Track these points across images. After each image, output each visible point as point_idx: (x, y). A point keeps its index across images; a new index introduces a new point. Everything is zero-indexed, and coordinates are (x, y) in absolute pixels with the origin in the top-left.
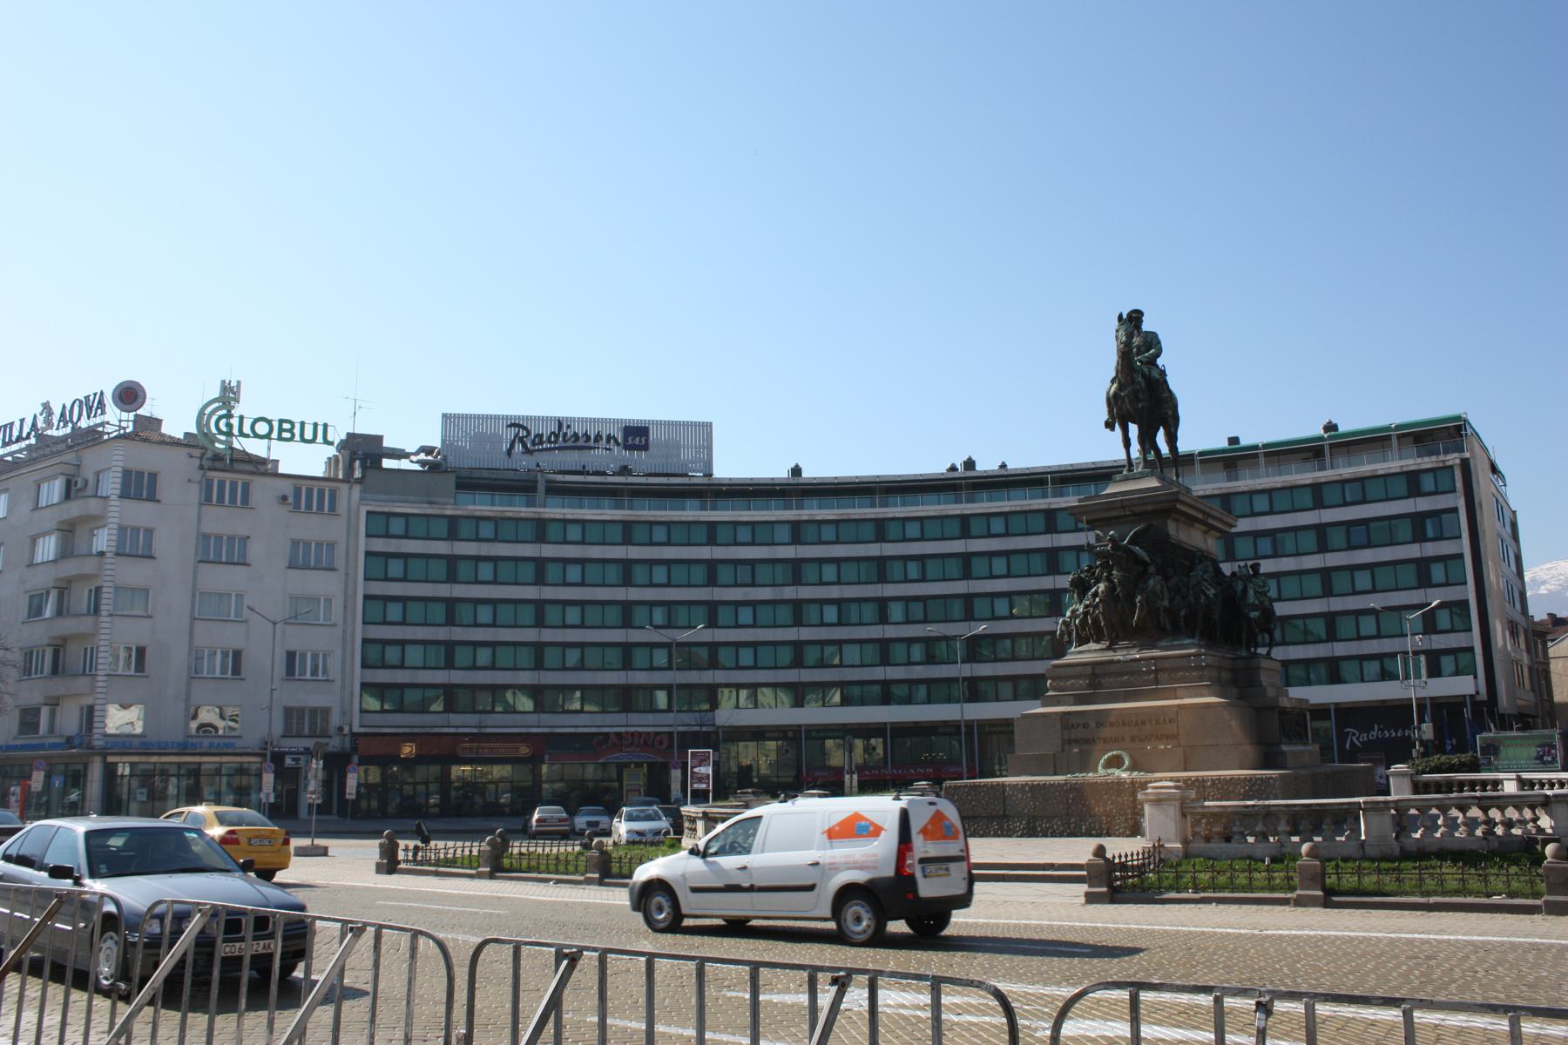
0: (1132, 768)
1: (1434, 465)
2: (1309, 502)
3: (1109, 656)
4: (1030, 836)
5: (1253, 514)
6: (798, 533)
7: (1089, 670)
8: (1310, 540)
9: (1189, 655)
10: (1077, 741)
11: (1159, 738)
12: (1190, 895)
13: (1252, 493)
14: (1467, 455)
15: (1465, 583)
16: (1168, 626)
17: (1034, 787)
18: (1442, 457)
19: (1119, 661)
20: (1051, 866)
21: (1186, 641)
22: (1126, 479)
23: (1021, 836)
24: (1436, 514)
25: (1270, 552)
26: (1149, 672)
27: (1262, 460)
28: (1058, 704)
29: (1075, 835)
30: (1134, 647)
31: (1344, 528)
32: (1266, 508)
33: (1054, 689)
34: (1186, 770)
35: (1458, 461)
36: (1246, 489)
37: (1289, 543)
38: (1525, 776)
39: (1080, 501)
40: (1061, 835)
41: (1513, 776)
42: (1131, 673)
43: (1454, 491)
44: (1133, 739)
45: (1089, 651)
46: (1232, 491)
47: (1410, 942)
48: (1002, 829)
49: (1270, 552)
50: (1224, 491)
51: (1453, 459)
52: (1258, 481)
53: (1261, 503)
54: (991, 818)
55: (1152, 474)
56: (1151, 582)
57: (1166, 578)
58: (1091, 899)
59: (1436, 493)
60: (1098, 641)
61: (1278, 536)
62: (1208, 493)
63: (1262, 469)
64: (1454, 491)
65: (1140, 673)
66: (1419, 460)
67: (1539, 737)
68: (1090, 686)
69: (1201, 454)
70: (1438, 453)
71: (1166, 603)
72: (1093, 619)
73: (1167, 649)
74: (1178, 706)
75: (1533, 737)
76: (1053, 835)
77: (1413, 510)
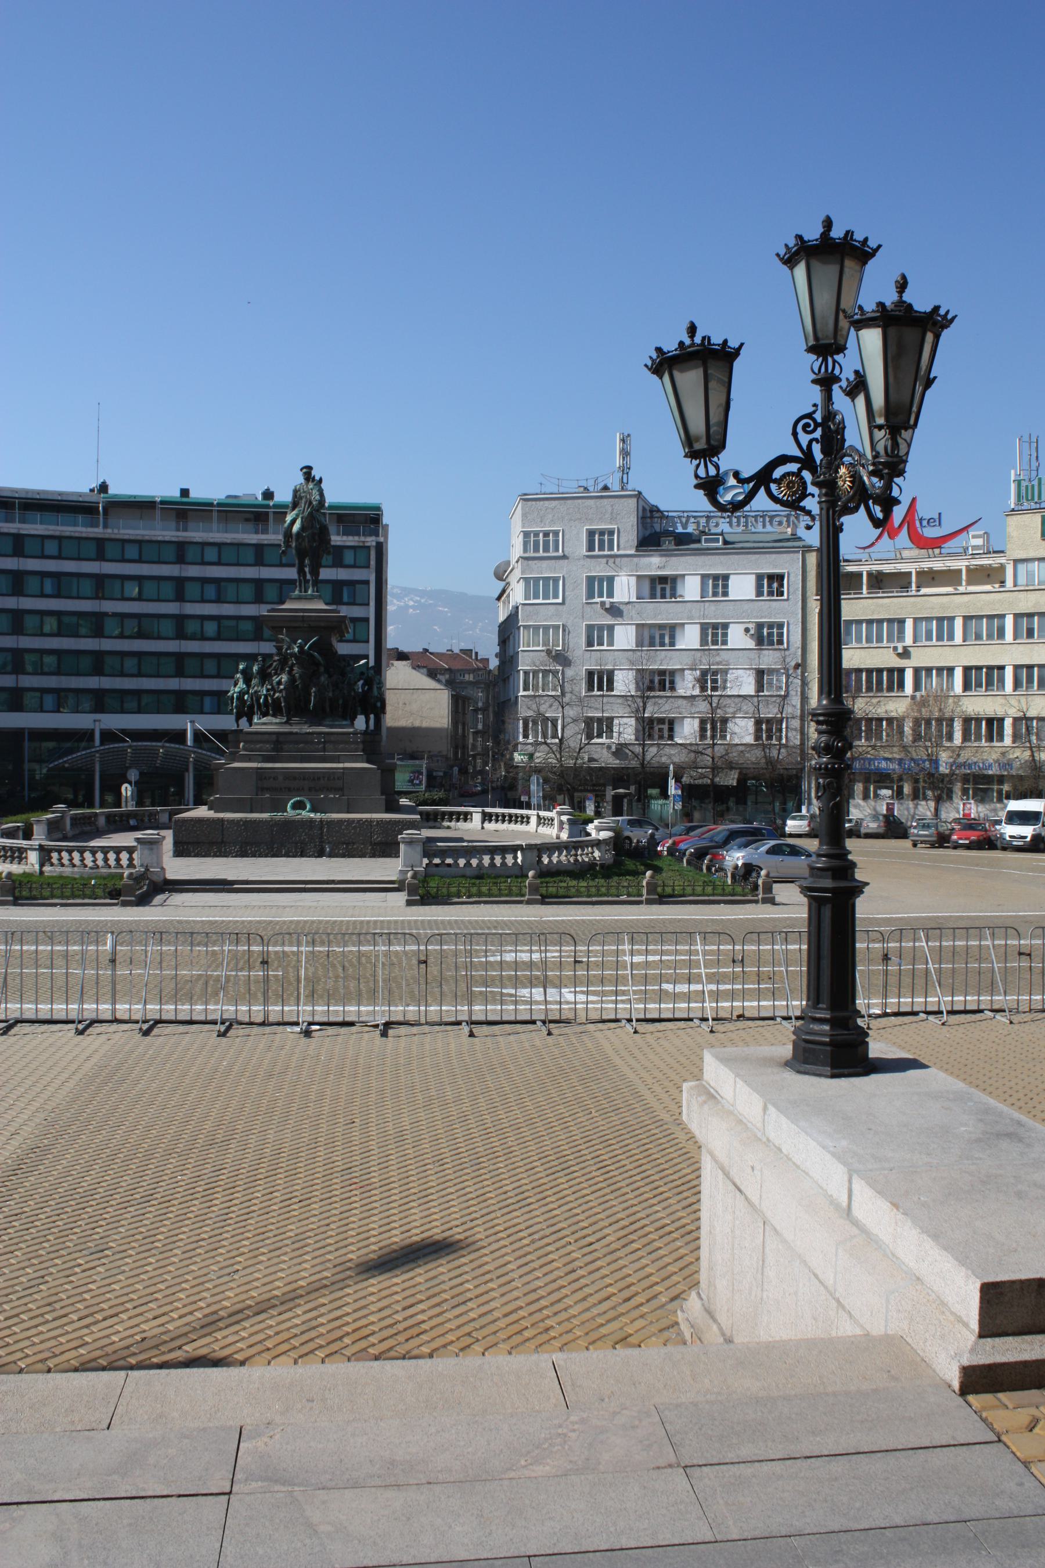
0: (313, 810)
1: (356, 544)
2: (251, 559)
3: (286, 729)
4: (243, 856)
5: (203, 563)
7: (274, 737)
8: (248, 591)
9: (349, 733)
10: (268, 789)
11: (330, 790)
12: (464, 899)
13: (204, 544)
14: (381, 539)
15: (367, 641)
16: (328, 710)
17: (247, 823)
18: (362, 539)
19: (296, 733)
20: (333, 882)
21: (344, 723)
22: (299, 598)
23: (236, 856)
24: (352, 583)
25: (213, 598)
26: (319, 742)
27: (215, 515)
28: (250, 760)
29: (277, 856)
30: (306, 723)
31: (278, 585)
32: (215, 559)
33: (245, 749)
34: (348, 812)
35: (374, 544)
36: (200, 540)
37: (231, 590)
38: (488, 810)
39: (269, 611)
40: (266, 856)
41: (480, 809)
42: (306, 742)
43: (368, 567)
44: (310, 789)
45: (271, 724)
46: (188, 540)
47: (243, 922)
48: (220, 852)
49: (213, 598)
50: (181, 539)
51: (371, 541)
52: (211, 535)
53: (211, 554)
54: (212, 843)
55: (320, 597)
56: (322, 679)
57: (330, 676)
58: (409, 903)
59: (354, 566)
60: (274, 715)
61: (223, 584)
62: (167, 539)
63: (215, 525)
64: (368, 567)
65: (312, 743)
66: (345, 538)
67: (413, 766)
68: (273, 750)
69: (162, 502)
70: (358, 535)
71: (330, 694)
72: (273, 700)
73: (331, 727)
74: (343, 768)
75: (408, 766)
76: (260, 856)
77: (334, 578)
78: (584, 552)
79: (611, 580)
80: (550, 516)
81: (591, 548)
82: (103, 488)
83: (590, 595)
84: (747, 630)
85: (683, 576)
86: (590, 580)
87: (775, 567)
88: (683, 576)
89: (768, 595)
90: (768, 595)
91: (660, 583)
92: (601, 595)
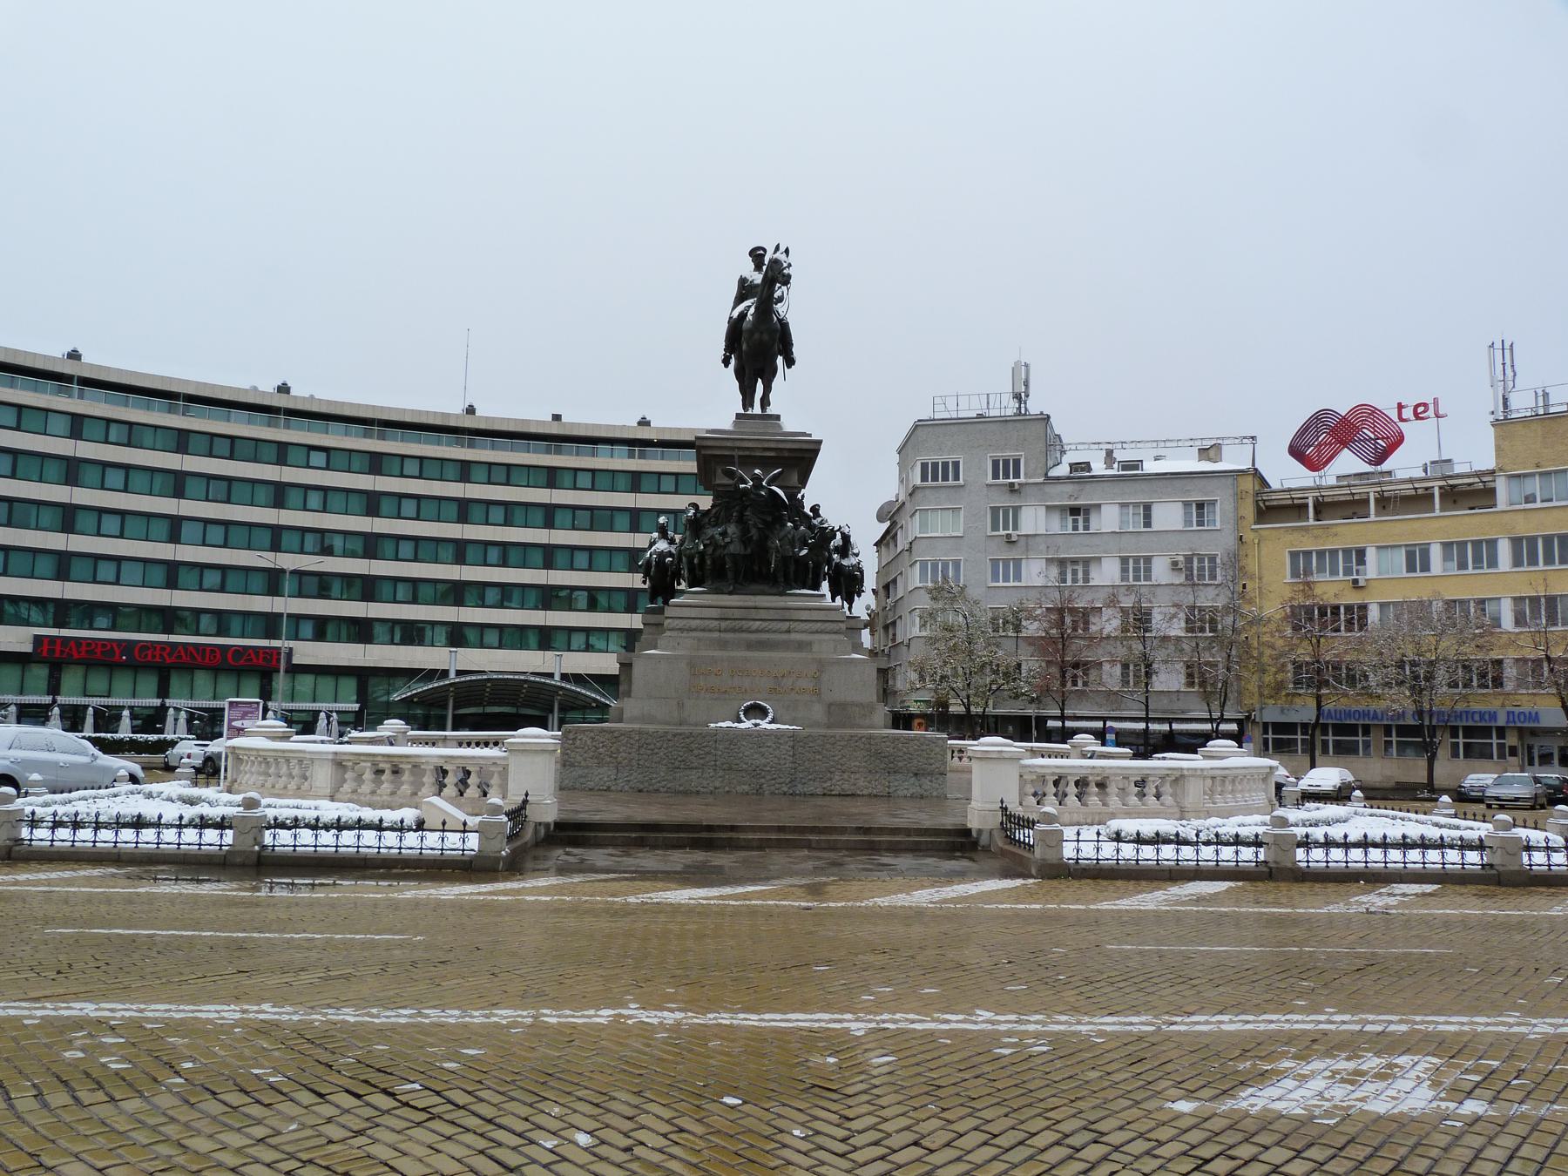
6: (77, 426)
78: (990, 480)
79: (1016, 510)
80: (950, 443)
81: (996, 476)
82: (471, 410)
83: (995, 527)
84: (1175, 564)
85: (1099, 506)
86: (995, 510)
87: (1206, 494)
88: (1099, 506)
89: (1198, 525)
90: (1198, 525)
91: (1071, 515)
92: (1006, 527)
